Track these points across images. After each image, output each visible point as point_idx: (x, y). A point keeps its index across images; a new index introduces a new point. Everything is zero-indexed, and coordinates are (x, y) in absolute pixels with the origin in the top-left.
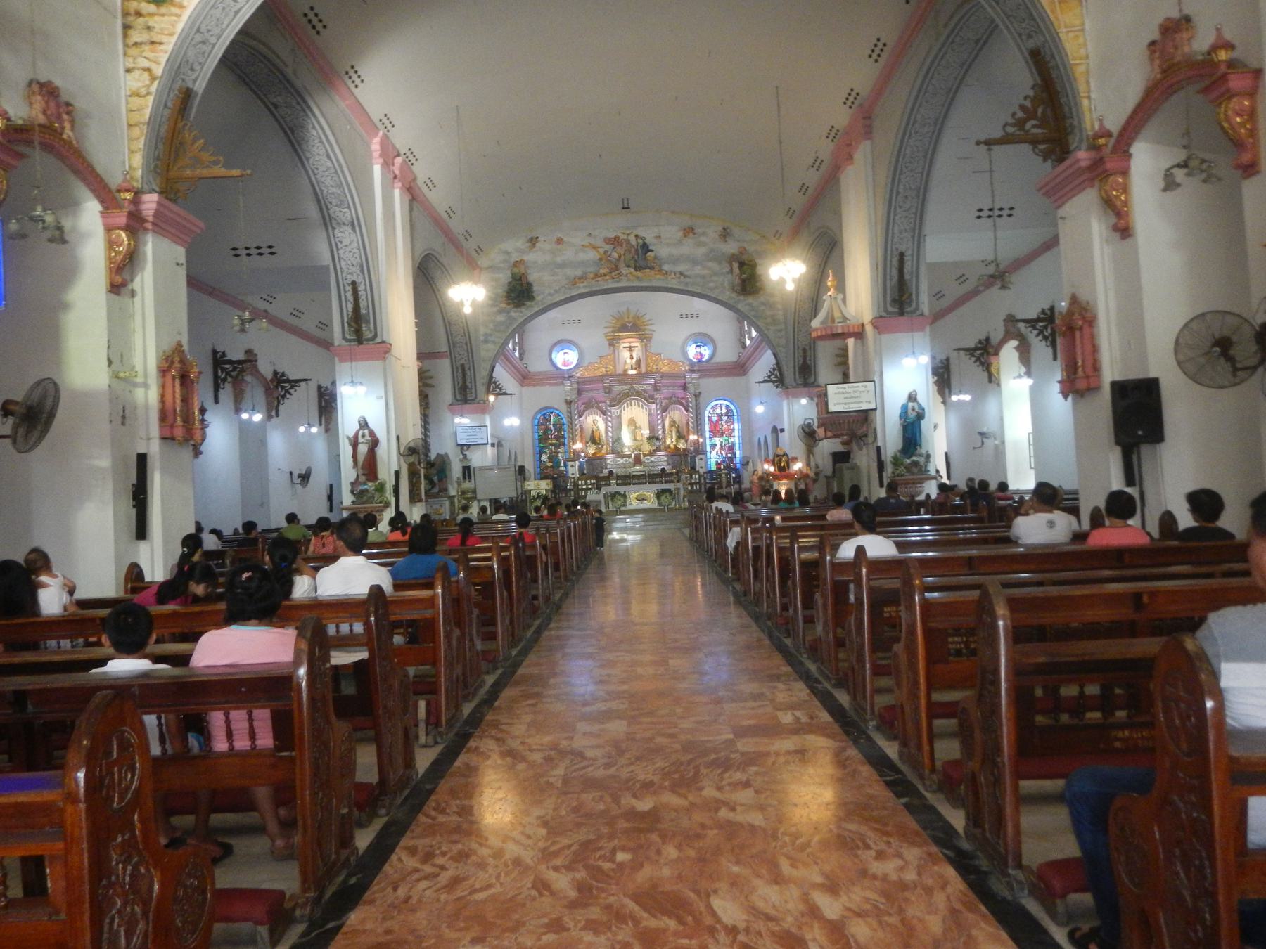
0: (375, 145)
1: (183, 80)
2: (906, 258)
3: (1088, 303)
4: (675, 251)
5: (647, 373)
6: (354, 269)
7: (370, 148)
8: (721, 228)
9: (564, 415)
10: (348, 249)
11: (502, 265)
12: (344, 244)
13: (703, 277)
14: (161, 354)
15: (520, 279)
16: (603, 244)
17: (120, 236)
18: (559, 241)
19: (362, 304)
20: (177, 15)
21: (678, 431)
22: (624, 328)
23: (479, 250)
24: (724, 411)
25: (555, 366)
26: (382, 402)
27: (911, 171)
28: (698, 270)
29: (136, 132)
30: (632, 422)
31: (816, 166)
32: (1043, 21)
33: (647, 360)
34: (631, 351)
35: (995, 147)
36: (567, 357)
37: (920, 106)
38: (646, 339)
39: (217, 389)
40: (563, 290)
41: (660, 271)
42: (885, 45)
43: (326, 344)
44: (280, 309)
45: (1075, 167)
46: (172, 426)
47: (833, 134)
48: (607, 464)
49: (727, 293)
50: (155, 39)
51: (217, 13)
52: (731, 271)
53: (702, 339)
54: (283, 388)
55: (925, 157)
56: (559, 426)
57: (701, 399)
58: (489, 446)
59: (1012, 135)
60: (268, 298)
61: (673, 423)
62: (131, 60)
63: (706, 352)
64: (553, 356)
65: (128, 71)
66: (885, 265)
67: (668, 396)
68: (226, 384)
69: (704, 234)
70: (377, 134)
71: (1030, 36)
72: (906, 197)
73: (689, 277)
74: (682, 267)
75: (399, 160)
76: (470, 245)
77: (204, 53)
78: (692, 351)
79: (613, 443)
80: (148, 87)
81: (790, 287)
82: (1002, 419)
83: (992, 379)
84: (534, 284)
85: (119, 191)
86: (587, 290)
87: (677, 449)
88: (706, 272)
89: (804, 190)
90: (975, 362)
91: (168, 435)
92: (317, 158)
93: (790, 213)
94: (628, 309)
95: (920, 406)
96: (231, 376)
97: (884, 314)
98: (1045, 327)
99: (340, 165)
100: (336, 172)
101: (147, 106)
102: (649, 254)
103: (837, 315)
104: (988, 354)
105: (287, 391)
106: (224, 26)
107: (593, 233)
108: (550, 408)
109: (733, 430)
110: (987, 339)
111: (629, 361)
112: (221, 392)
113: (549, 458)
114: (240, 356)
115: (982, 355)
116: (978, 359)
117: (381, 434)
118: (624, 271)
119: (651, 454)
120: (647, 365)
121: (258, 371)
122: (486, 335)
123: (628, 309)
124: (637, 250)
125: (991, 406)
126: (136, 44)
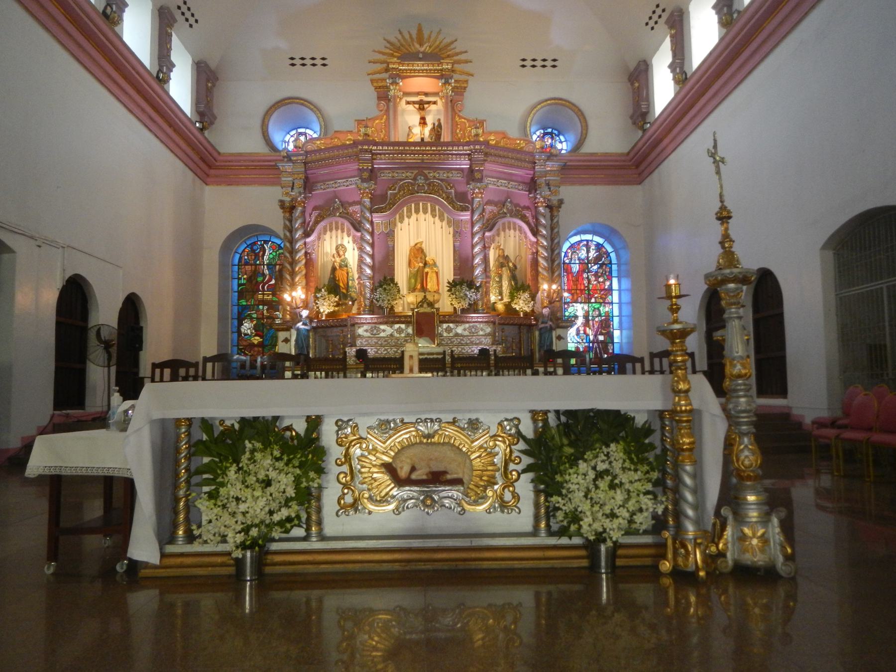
21: (513, 277)
22: (409, 56)
24: (593, 254)
30: (418, 252)
33: (453, 133)
48: (355, 337)
57: (563, 215)
61: (504, 261)
67: (496, 199)
79: (373, 290)
94: (420, 30)
109: (610, 290)
111: (417, 130)
113: (255, 328)
119: (455, 318)
123: (420, 30)
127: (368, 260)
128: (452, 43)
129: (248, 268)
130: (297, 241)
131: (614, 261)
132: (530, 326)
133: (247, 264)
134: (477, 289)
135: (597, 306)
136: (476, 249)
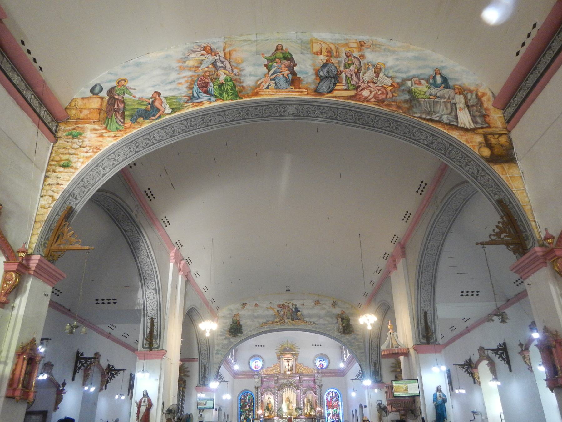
0: (172, 254)
1: (70, 203)
2: (428, 315)
3: (556, 331)
4: (311, 312)
5: (295, 373)
6: (153, 311)
7: (170, 255)
8: (332, 302)
9: (254, 394)
10: (152, 302)
11: (228, 316)
12: (150, 299)
13: (324, 325)
14: (20, 345)
15: (236, 323)
16: (276, 307)
17: (11, 275)
18: (256, 305)
19: (155, 329)
20: (73, 173)
21: (311, 405)
23: (218, 308)
24: (334, 395)
25: (251, 368)
26: (157, 383)
27: (427, 271)
28: (321, 321)
29: (38, 225)
30: (288, 399)
31: (378, 272)
32: (503, 185)
34: (288, 362)
35: (487, 246)
36: (257, 363)
37: (430, 240)
38: (295, 356)
39: (75, 372)
40: (256, 329)
41: (303, 321)
42: (410, 214)
43: (134, 350)
44: (117, 332)
45: (534, 256)
46: (15, 390)
47: (386, 256)
49: (336, 333)
50: (60, 183)
51: (94, 174)
52: (338, 322)
53: (323, 357)
54: (111, 374)
55: (434, 265)
56: (251, 400)
57: (323, 388)
58: (214, 410)
59: (494, 240)
60: (112, 327)
62: (45, 191)
63: (325, 364)
64: (251, 363)
65: (42, 196)
66: (418, 319)
68: (80, 370)
69: (325, 304)
70: (173, 249)
71: (496, 194)
72: (426, 284)
73: (317, 324)
74: (314, 320)
75: (183, 262)
76: (214, 306)
77: (83, 192)
78: (318, 363)
79: (278, 410)
80: (50, 204)
81: (370, 328)
82: (484, 404)
83: (476, 381)
84: (243, 326)
85: (18, 252)
86: (268, 329)
87: (310, 414)
88: (325, 322)
89: (372, 283)
90: (465, 372)
91: (11, 395)
92: (143, 257)
93: (365, 295)
94: (287, 341)
95: (444, 395)
96: (84, 366)
97: (420, 343)
98: (503, 353)
99: (153, 260)
100: (151, 264)
101: (46, 213)
102: (298, 313)
103: (394, 343)
104: (472, 368)
105: (113, 376)
106: (96, 181)
107: (272, 302)
108: (247, 390)
109: (339, 405)
110: (470, 360)
111: (287, 367)
112: (77, 376)
114: (91, 355)
115: (468, 368)
116: (466, 370)
117: (154, 401)
118: (286, 321)
119: (297, 417)
120: (296, 369)
121: (99, 364)
122: (217, 350)
123: (287, 341)
124: (292, 311)
125: (476, 397)
126: (49, 184)
127: (277, 403)
128: (294, 345)
129: (243, 400)
130: (259, 397)
131: (340, 397)
132: (315, 419)
133: (243, 399)
134: (302, 410)
135: (335, 410)
136: (302, 400)
